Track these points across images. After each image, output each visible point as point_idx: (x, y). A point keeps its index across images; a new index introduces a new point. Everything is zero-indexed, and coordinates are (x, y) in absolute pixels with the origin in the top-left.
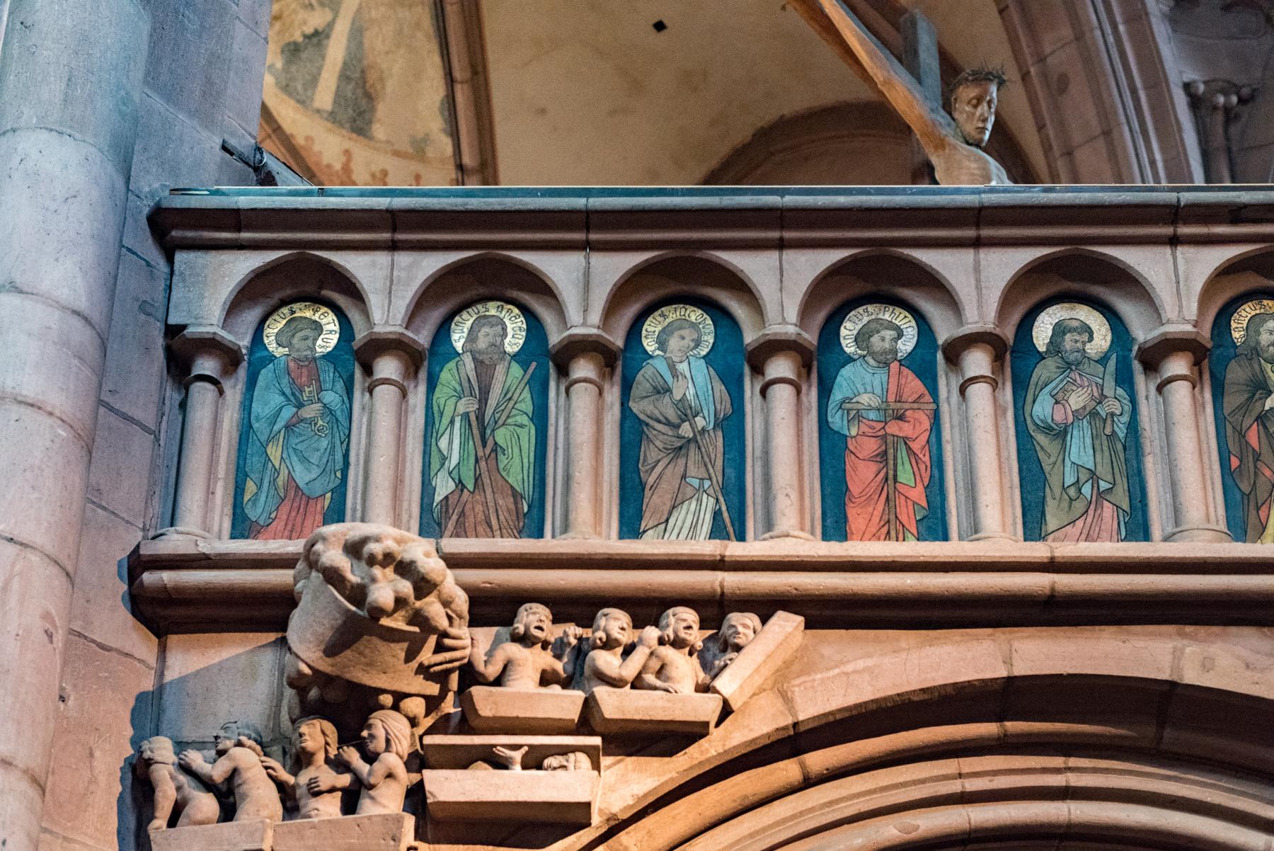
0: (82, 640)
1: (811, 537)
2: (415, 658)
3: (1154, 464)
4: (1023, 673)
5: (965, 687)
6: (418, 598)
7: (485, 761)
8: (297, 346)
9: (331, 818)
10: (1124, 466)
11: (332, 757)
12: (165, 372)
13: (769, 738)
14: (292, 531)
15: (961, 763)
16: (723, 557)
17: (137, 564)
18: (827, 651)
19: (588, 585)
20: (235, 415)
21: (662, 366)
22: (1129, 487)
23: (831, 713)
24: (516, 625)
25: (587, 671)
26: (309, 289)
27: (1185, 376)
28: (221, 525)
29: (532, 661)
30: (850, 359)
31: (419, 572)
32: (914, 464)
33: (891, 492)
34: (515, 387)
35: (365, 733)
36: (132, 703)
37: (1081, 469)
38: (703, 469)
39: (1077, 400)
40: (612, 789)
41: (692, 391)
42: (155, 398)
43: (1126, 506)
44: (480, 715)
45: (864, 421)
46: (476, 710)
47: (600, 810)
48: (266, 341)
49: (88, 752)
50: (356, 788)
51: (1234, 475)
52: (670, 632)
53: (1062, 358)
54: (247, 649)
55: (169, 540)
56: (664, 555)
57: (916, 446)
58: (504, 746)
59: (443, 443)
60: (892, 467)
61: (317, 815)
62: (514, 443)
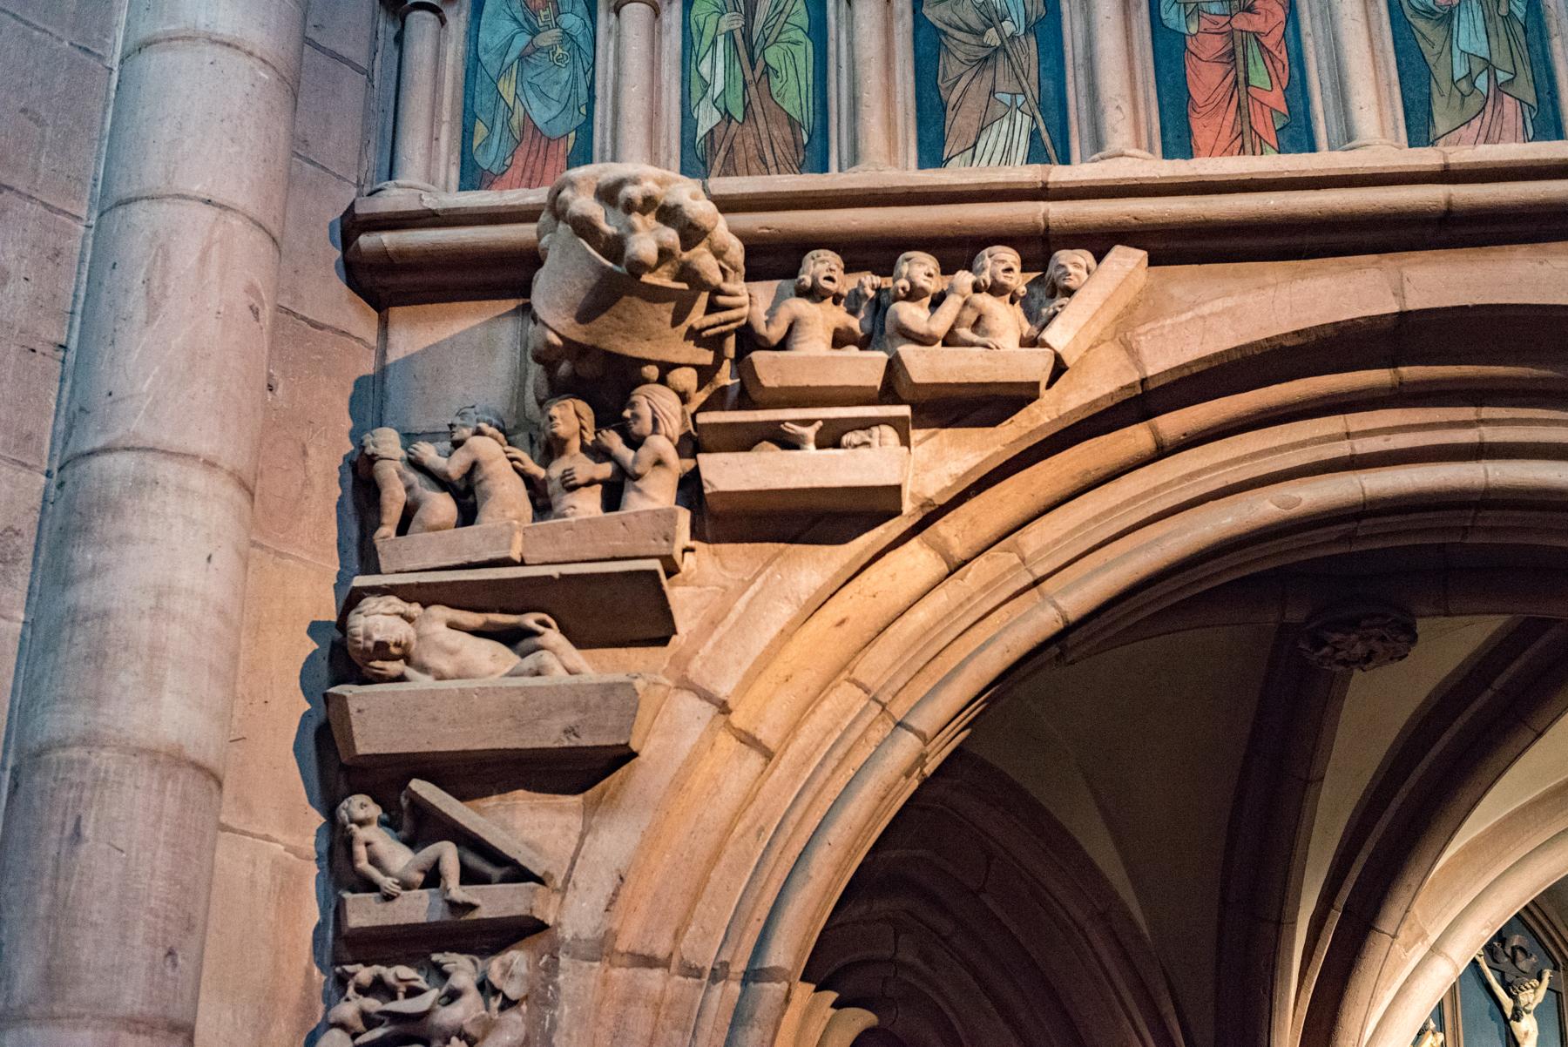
1: (1150, 156)
4: (1419, 306)
5: (1349, 327)
6: (686, 248)
9: (591, 516)
10: (1526, 53)
11: (589, 443)
14: (530, 179)
15: (1348, 420)
16: (1045, 184)
17: (352, 226)
18: (1177, 291)
19: (885, 225)
22: (1533, 76)
23: (1186, 366)
24: (801, 277)
25: (889, 327)
28: (447, 177)
29: (822, 319)
35: (627, 413)
36: (350, 390)
37: (1473, 58)
38: (1015, 82)
40: (926, 469)
42: (368, 32)
43: (1531, 99)
44: (763, 386)
45: (1205, 15)
46: (758, 380)
47: (913, 495)
50: (618, 479)
52: (986, 277)
54: (483, 320)
55: (388, 196)
57: (1269, 42)
59: (705, 68)
61: (573, 514)
62: (788, 62)
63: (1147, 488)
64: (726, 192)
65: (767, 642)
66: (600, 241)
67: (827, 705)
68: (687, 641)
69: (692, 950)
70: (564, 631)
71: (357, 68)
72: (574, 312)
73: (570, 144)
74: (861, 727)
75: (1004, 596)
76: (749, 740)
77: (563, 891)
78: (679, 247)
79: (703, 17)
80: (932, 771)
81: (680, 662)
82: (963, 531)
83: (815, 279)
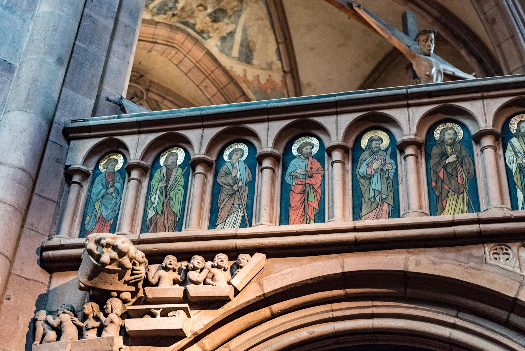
0: (19, 277)
3: (403, 187)
4: (348, 271)
5: (327, 277)
7: (148, 314)
8: (109, 168)
9: (93, 338)
10: (392, 189)
11: (95, 315)
12: (64, 181)
18: (276, 266)
21: (229, 165)
26: (115, 148)
27: (412, 154)
29: (168, 277)
30: (295, 157)
32: (315, 193)
33: (306, 205)
35: (105, 307)
36: (37, 298)
38: (240, 201)
39: (376, 165)
41: (239, 173)
43: (392, 204)
45: (298, 179)
48: (100, 167)
51: (434, 189)
53: (371, 150)
56: (215, 235)
57: (316, 187)
58: (154, 309)
59: (153, 199)
60: (307, 195)
61: (87, 337)
64: (145, 238)
66: (95, 256)
71: (53, 201)
72: (87, 277)
73: (112, 222)
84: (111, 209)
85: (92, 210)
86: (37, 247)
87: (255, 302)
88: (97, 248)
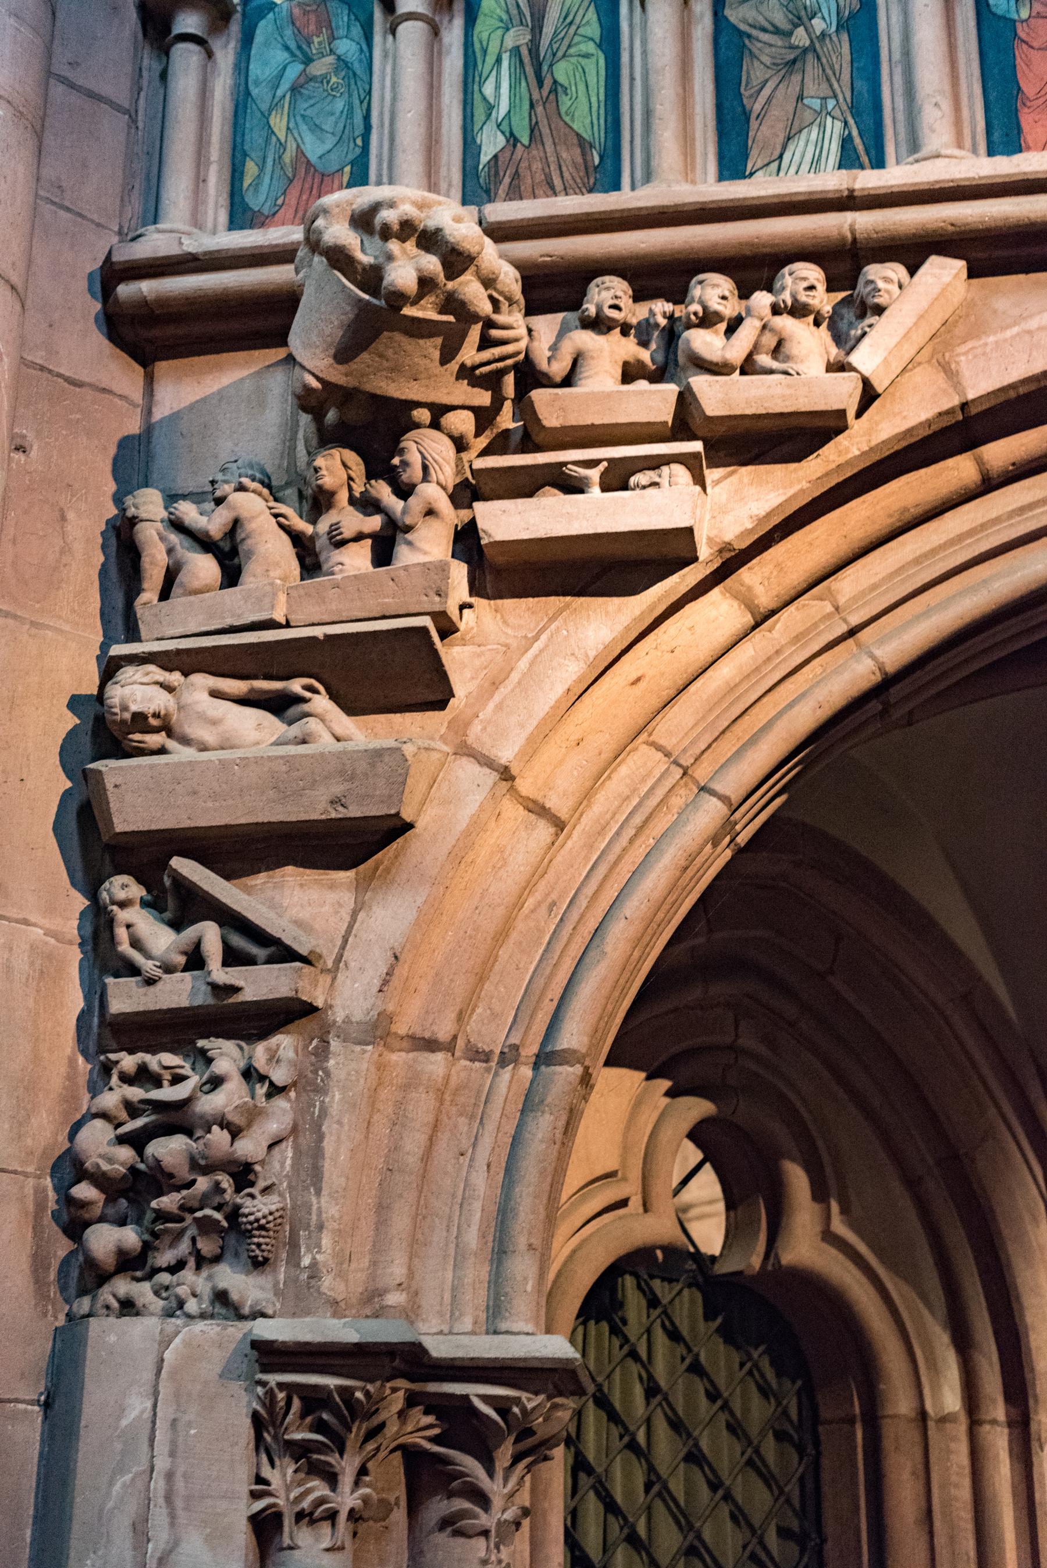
0: (46, 375)
2: (453, 358)
6: (451, 275)
11: (357, 495)
12: (140, 36)
13: (930, 426)
16: (851, 191)
18: (1001, 304)
19: (676, 245)
20: (228, 81)
24: (585, 306)
25: (681, 359)
28: (215, 219)
31: (447, 242)
34: (577, 6)
35: (396, 461)
36: (113, 451)
38: (825, 86)
40: (724, 510)
42: (128, 68)
44: (544, 427)
46: (538, 420)
47: (710, 540)
49: (57, 514)
50: (390, 533)
52: (787, 297)
54: (252, 371)
56: (774, 196)
59: (488, 89)
61: (341, 571)
62: (578, 77)
63: (974, 525)
65: (552, 703)
66: (355, 272)
67: (624, 770)
68: (466, 704)
69: (479, 1033)
70: (334, 697)
71: (119, 108)
72: (332, 351)
74: (660, 793)
75: (816, 647)
76: (538, 809)
77: (334, 971)
78: (442, 275)
79: (487, 33)
80: (746, 840)
81: (458, 727)
82: (769, 579)
83: (599, 309)
84: (333, 133)
85: (261, 141)
86: (89, 270)
87: (931, 432)
88: (362, 241)
